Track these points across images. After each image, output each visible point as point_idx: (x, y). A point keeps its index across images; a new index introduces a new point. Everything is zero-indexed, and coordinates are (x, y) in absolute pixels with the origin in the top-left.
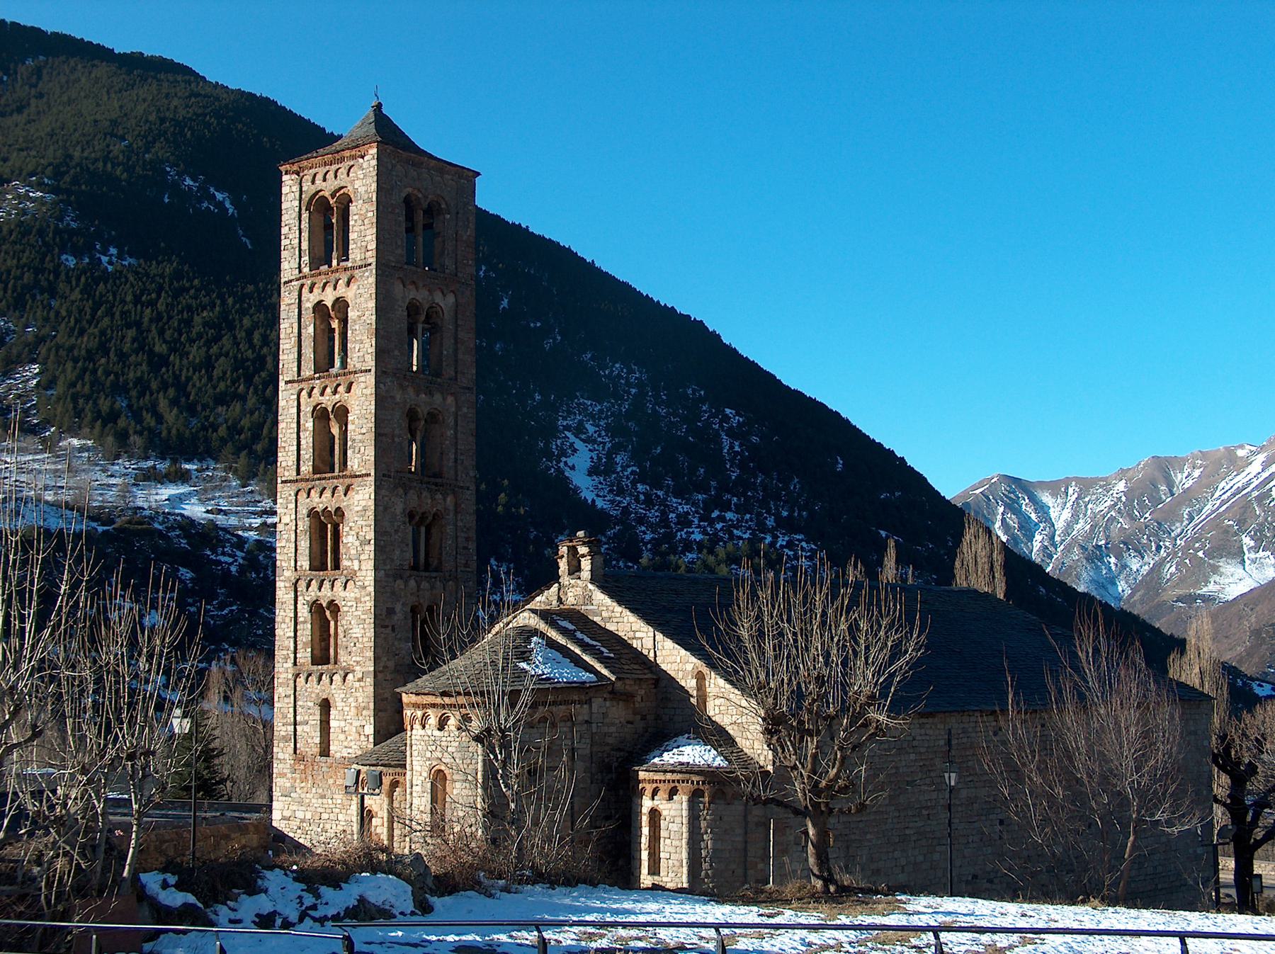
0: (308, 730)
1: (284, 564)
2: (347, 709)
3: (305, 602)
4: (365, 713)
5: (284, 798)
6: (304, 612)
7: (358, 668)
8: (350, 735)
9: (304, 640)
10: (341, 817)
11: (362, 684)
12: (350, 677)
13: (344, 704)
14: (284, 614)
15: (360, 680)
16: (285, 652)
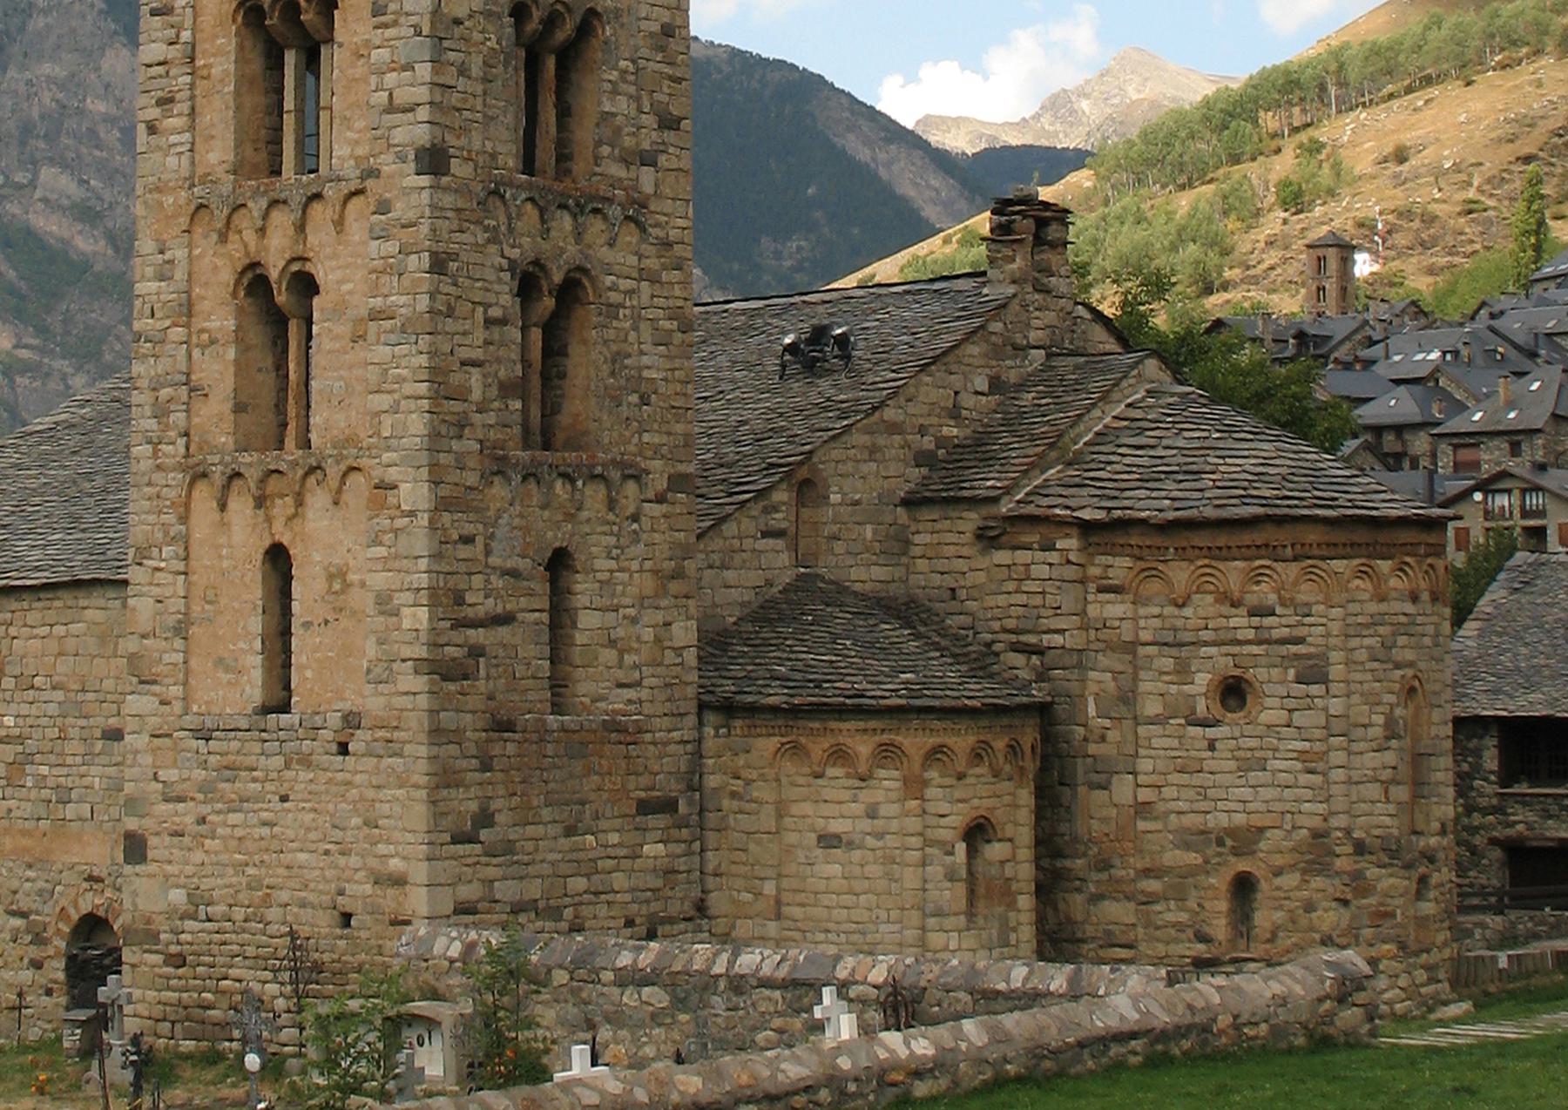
0: (517, 640)
1: (451, 139)
2: (624, 576)
3: (505, 263)
4: (674, 587)
5: (460, 849)
6: (505, 299)
7: (657, 464)
8: (630, 650)
9: (502, 373)
10: (619, 880)
11: (664, 508)
12: (631, 488)
13: (613, 564)
14: (451, 289)
15: (660, 499)
16: (456, 406)
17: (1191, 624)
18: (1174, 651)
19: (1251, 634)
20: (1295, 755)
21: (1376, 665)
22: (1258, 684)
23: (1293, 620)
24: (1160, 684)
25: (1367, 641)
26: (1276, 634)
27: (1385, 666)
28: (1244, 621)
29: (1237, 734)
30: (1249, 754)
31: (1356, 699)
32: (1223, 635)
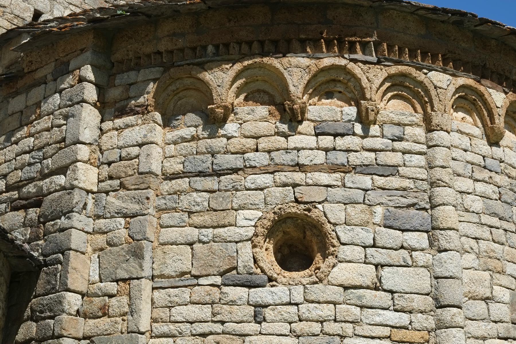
17: (236, 144)
18: (211, 183)
19: (320, 157)
20: (386, 331)
21: (495, 221)
22: (328, 227)
23: (378, 143)
24: (188, 230)
25: (480, 187)
26: (355, 159)
27: (505, 225)
28: (312, 141)
29: (298, 295)
30: (316, 328)
31: (470, 259)
32: (280, 157)
